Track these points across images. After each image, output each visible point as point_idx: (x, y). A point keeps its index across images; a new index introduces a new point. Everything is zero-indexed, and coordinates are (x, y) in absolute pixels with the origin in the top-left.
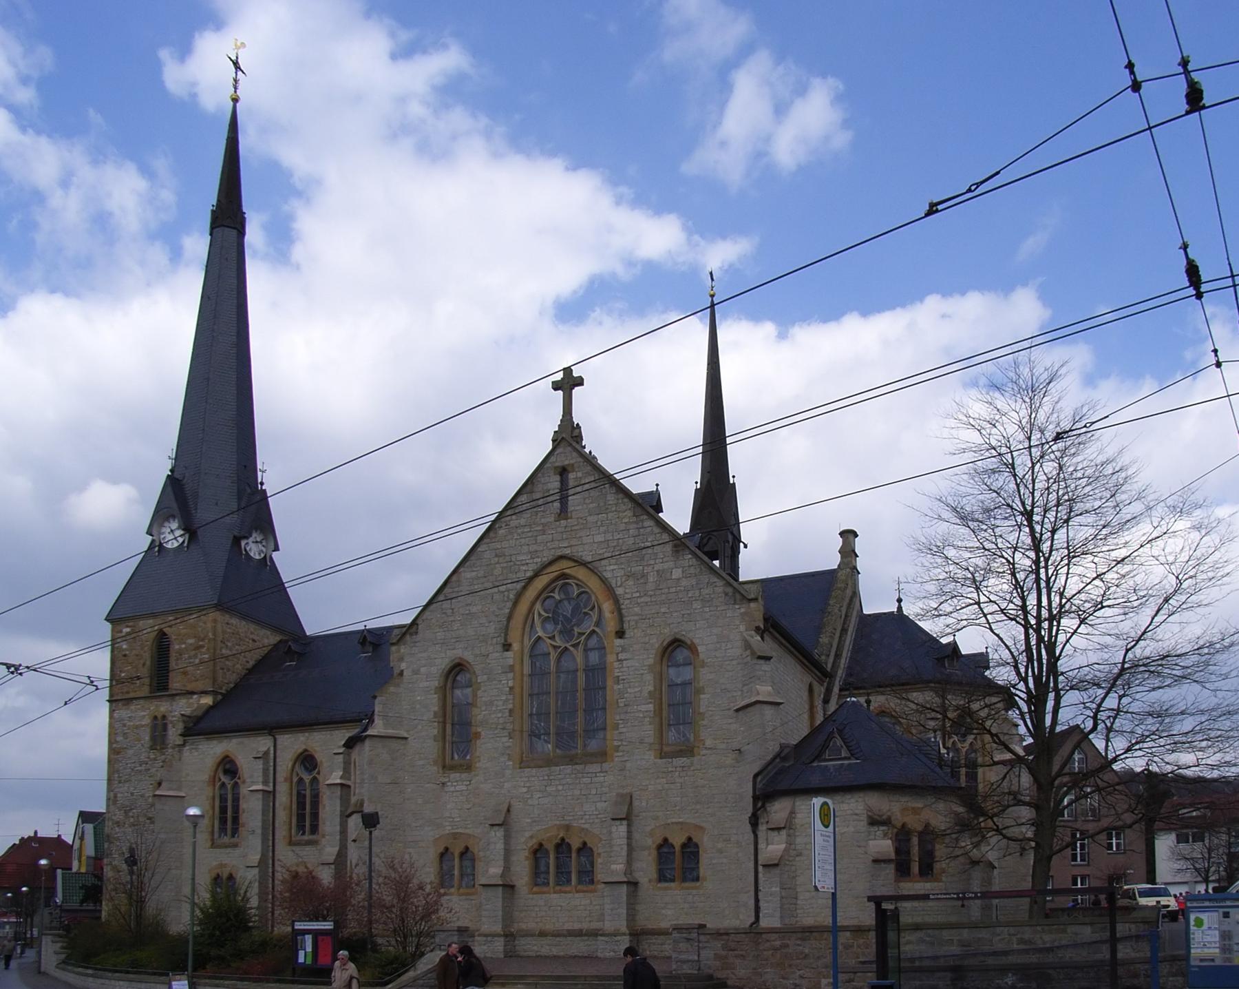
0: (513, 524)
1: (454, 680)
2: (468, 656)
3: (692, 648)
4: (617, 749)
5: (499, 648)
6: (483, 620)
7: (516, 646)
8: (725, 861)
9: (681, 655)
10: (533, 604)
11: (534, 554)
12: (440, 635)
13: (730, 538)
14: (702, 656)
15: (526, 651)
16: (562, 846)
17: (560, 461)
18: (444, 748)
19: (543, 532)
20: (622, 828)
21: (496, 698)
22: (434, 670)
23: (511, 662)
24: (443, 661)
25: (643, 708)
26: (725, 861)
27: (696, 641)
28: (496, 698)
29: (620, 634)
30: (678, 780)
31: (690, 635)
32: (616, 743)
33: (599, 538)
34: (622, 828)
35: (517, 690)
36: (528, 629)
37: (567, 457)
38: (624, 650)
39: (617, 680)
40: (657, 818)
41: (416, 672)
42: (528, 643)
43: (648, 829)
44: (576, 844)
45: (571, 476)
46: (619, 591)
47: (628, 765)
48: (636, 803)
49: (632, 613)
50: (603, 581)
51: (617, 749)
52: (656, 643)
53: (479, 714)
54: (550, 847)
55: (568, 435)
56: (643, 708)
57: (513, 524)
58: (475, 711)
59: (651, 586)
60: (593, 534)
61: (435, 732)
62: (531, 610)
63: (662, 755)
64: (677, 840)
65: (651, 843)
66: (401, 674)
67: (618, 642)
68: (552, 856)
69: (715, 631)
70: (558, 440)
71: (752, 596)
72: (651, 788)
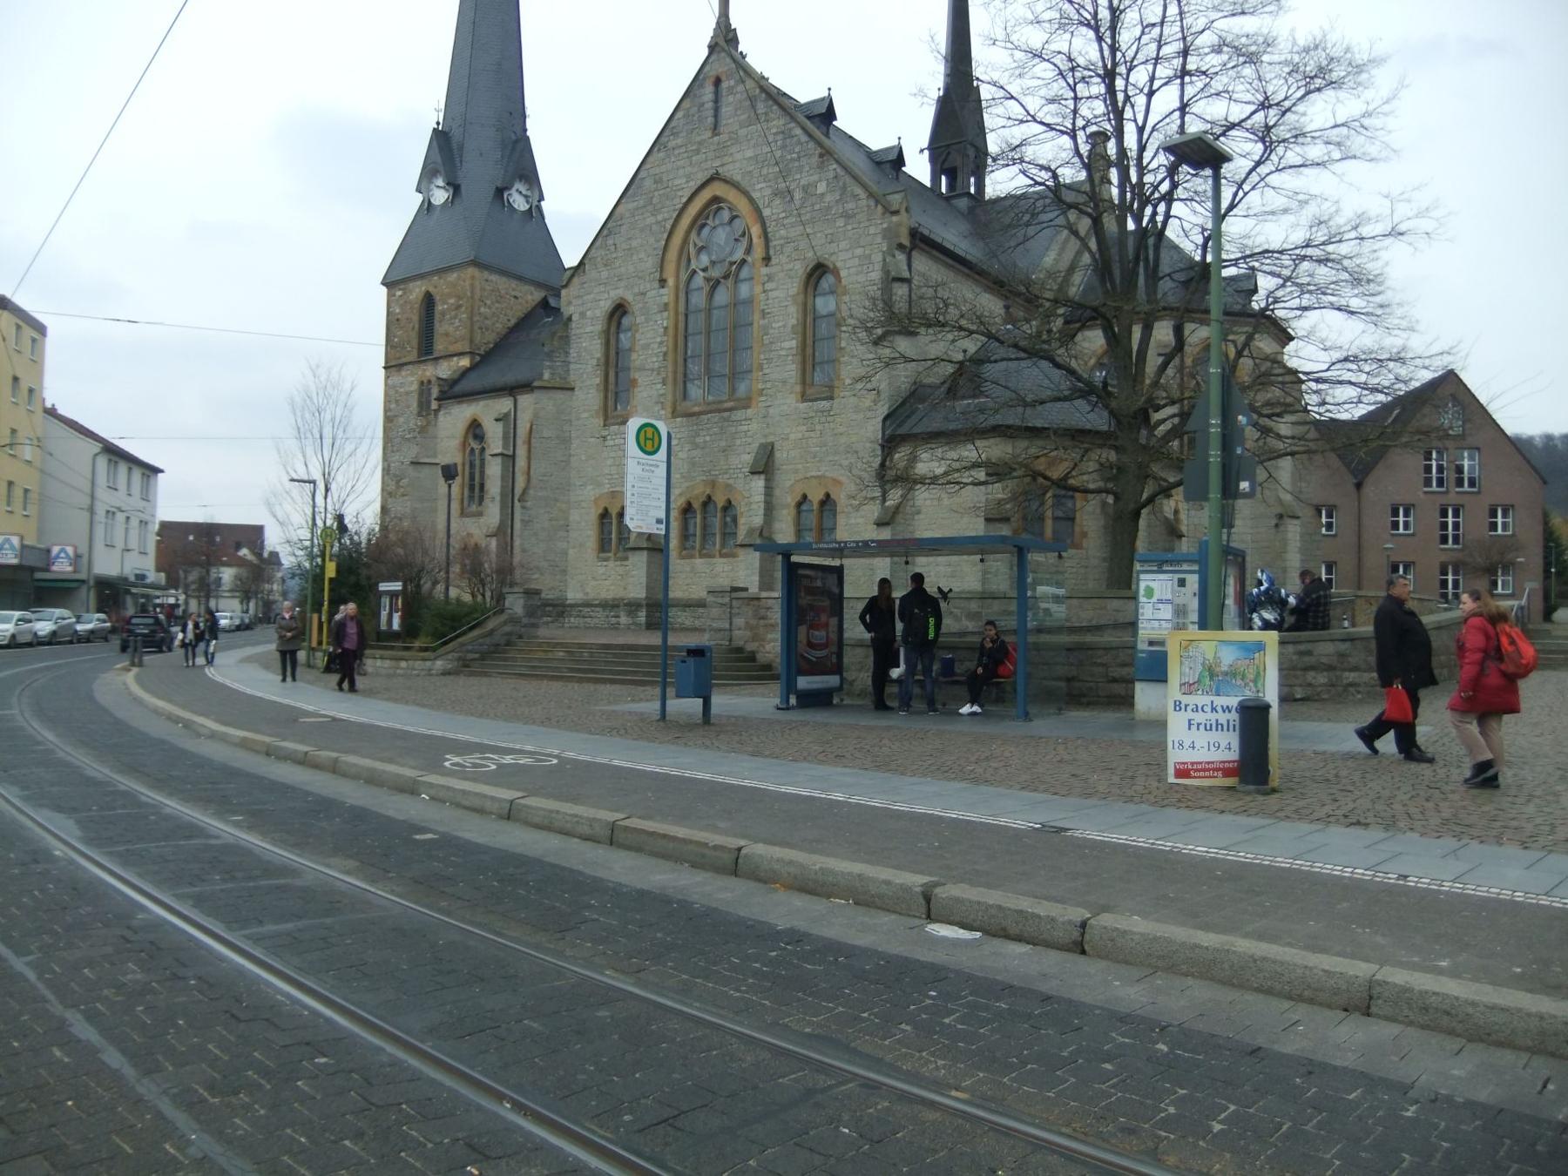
0: (670, 145)
1: (619, 324)
2: (629, 298)
3: (836, 272)
4: (761, 392)
5: (656, 285)
6: (642, 255)
7: (671, 282)
8: (860, 520)
9: (827, 282)
10: (688, 232)
11: (689, 178)
12: (605, 274)
13: (971, 152)
14: (844, 282)
15: (681, 286)
16: (708, 502)
17: (712, 71)
18: (606, 397)
19: (698, 152)
20: (759, 483)
21: (650, 339)
22: (598, 313)
23: (665, 299)
24: (606, 305)
25: (787, 345)
26: (860, 520)
27: (839, 264)
28: (650, 339)
29: (767, 259)
30: (818, 427)
31: (833, 258)
32: (760, 386)
33: (749, 153)
34: (759, 483)
35: (671, 331)
36: (684, 263)
37: (722, 66)
38: (770, 278)
39: (764, 314)
40: (796, 472)
41: (583, 315)
42: (684, 277)
43: (788, 484)
44: (720, 501)
45: (724, 85)
46: (766, 212)
47: (771, 411)
48: (778, 455)
49: (778, 234)
50: (751, 200)
51: (761, 392)
52: (800, 269)
53: (637, 359)
54: (696, 505)
55: (725, 39)
56: (787, 345)
57: (670, 145)
58: (634, 356)
59: (798, 203)
60: (746, 154)
61: (598, 380)
62: (685, 241)
63: (804, 398)
64: (816, 496)
65: (791, 500)
66: (570, 319)
67: (765, 270)
68: (699, 516)
69: (859, 251)
70: (713, 48)
71: (894, 208)
72: (792, 436)
